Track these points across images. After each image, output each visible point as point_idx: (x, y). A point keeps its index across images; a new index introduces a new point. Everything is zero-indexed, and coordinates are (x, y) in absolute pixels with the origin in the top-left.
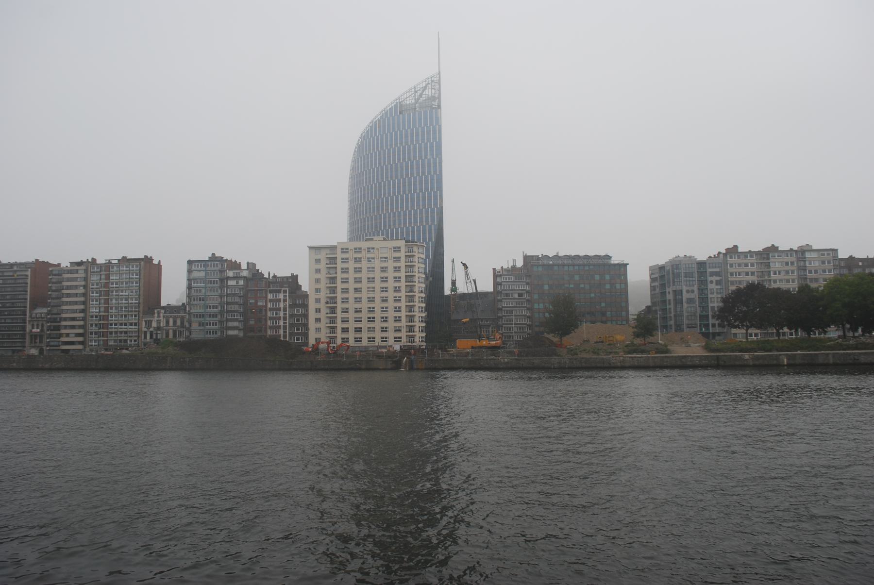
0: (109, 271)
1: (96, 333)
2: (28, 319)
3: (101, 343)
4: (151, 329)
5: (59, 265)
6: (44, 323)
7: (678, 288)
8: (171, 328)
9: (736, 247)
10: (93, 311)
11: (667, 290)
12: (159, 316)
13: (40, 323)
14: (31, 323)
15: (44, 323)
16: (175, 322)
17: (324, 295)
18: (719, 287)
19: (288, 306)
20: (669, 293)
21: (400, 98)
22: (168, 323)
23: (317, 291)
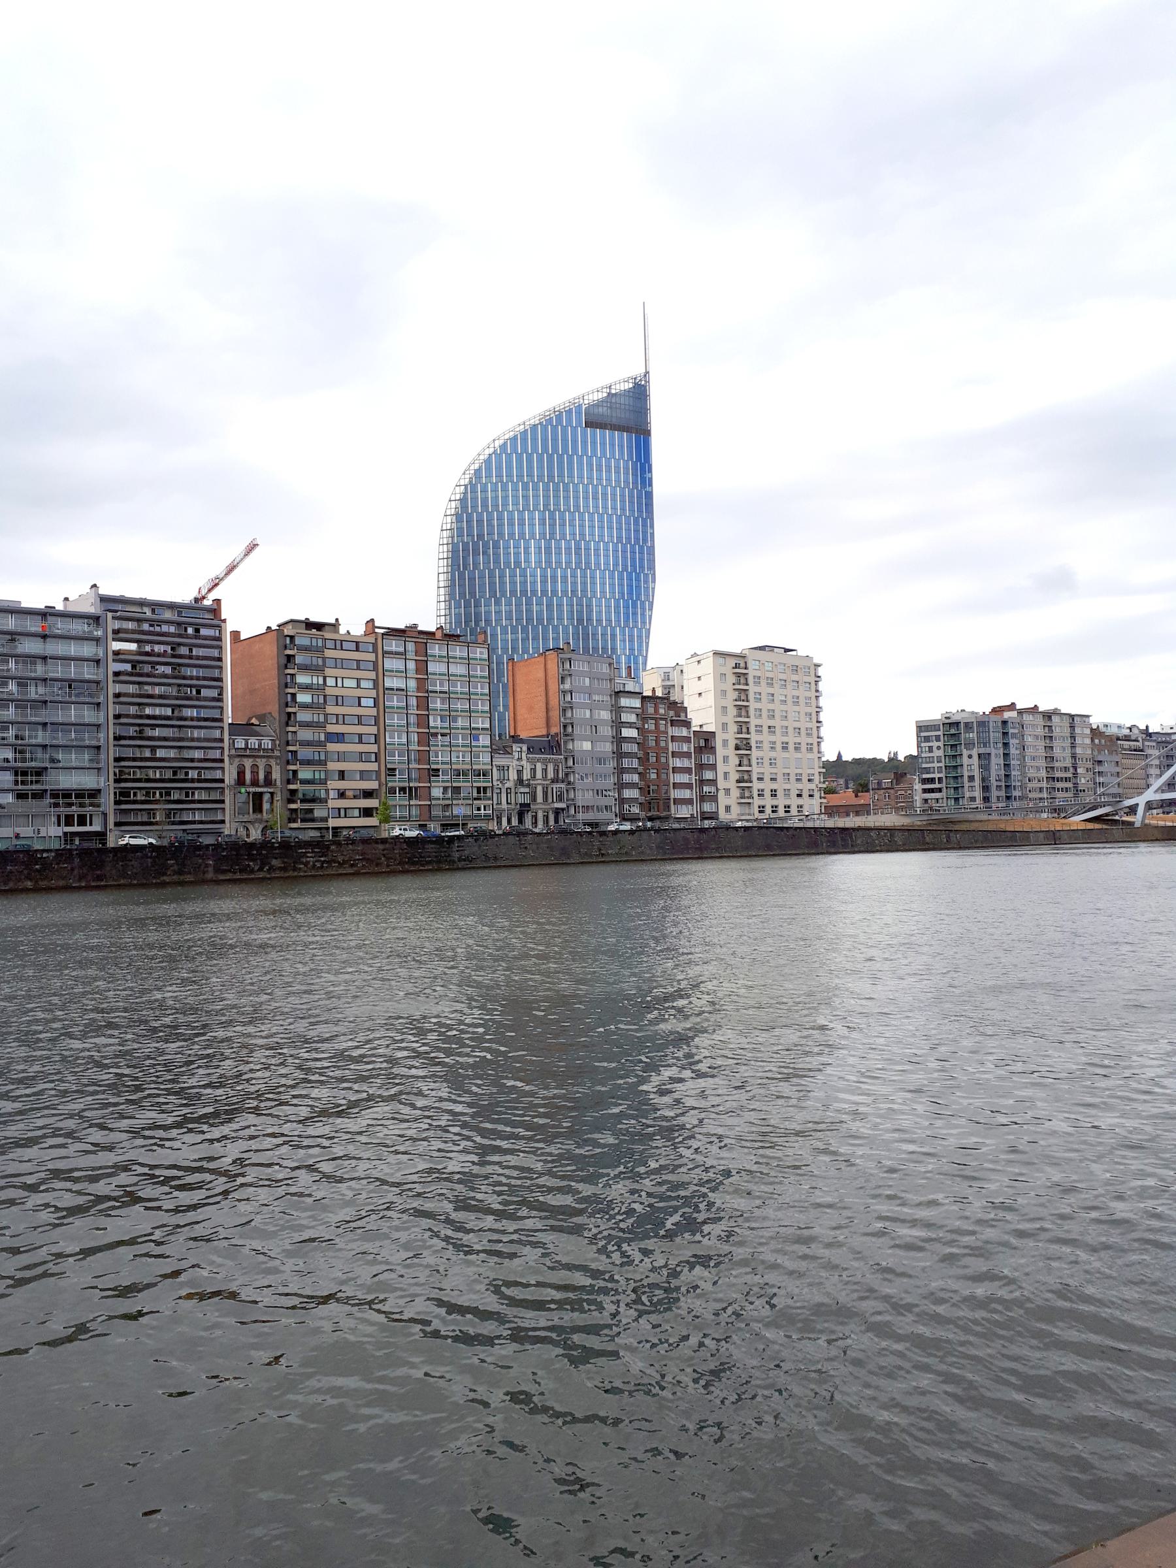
0: (426, 656)
1: (402, 789)
2: (226, 752)
3: (414, 812)
4: (508, 785)
5: (335, 626)
6: (273, 762)
7: (987, 750)
8: (539, 782)
9: (1013, 704)
10: (395, 739)
11: (965, 753)
12: (520, 759)
13: (261, 763)
14: (237, 761)
15: (273, 762)
16: (545, 770)
17: (731, 736)
18: (1018, 752)
19: (693, 751)
20: (970, 757)
21: (586, 397)
22: (534, 770)
23: (725, 726)
